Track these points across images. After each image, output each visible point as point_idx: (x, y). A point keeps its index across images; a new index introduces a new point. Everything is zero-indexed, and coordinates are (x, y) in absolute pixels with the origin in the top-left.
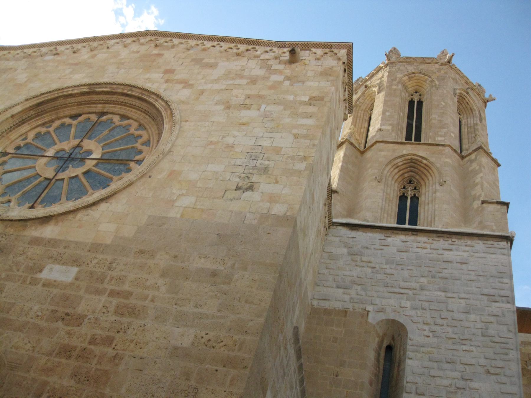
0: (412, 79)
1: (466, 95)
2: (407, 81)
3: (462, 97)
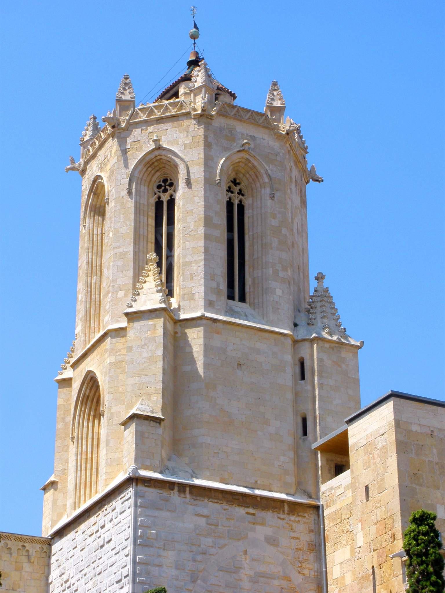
0: (98, 191)
1: (157, 153)
2: (95, 200)
3: (157, 161)
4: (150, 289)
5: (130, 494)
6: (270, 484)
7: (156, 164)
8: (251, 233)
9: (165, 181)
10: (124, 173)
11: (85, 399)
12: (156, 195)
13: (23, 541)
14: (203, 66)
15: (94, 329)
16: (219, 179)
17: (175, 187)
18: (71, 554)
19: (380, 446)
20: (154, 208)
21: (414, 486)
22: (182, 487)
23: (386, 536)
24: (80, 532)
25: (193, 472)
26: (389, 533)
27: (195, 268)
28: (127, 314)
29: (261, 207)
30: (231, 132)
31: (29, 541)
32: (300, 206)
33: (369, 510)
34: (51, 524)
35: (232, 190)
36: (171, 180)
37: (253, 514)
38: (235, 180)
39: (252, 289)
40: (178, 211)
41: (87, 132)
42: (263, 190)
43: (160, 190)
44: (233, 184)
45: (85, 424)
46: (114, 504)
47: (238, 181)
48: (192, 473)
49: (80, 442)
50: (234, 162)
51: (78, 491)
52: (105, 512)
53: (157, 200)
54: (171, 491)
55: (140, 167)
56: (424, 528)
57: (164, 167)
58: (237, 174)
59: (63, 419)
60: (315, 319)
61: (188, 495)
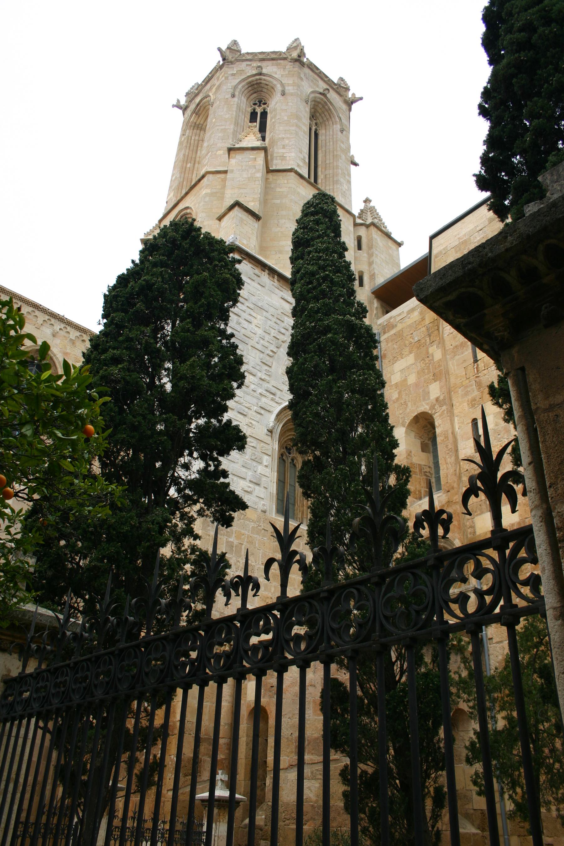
0: (200, 112)
1: (258, 77)
3: (257, 84)
9: (260, 102)
39: (324, 181)
42: (335, 126)
55: (243, 84)
57: (262, 91)
61: (276, 281)
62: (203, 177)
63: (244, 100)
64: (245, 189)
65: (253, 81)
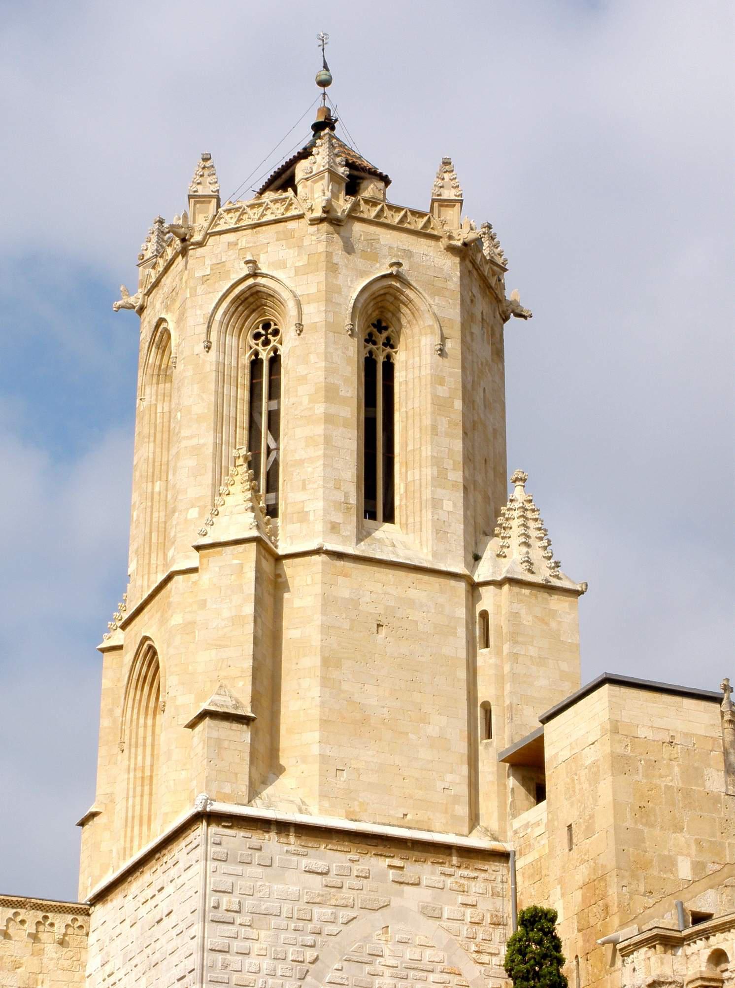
1: (251, 281)
3: (252, 295)
4: (237, 505)
5: (199, 839)
6: (429, 819)
7: (251, 300)
8: (403, 409)
9: (266, 326)
10: (200, 315)
11: (141, 679)
12: (252, 350)
13: (45, 909)
14: (326, 138)
15: (157, 567)
16: (351, 324)
17: (281, 337)
18: (118, 931)
19: (588, 762)
20: (247, 371)
21: (640, 827)
22: (282, 827)
23: (595, 909)
24: (130, 897)
25: (303, 802)
26: (601, 903)
27: (310, 470)
28: (198, 548)
29: (420, 367)
30: (372, 245)
31: (54, 910)
32: (489, 360)
33: (573, 864)
34: (91, 882)
35: (374, 338)
36: (275, 324)
37: (402, 868)
38: (379, 321)
40: (285, 377)
41: (149, 244)
43: (257, 342)
44: (375, 330)
45: (142, 721)
46: (177, 854)
47: (384, 324)
48: (301, 804)
49: (133, 750)
50: (377, 294)
51: (129, 830)
52: (165, 867)
53: (253, 357)
54: (265, 834)
56: (535, 935)
58: (382, 312)
59: (111, 711)
60: (508, 547)
61: (292, 839)
62: (169, 578)
63: (231, 341)
64: (227, 646)
65: (243, 292)
